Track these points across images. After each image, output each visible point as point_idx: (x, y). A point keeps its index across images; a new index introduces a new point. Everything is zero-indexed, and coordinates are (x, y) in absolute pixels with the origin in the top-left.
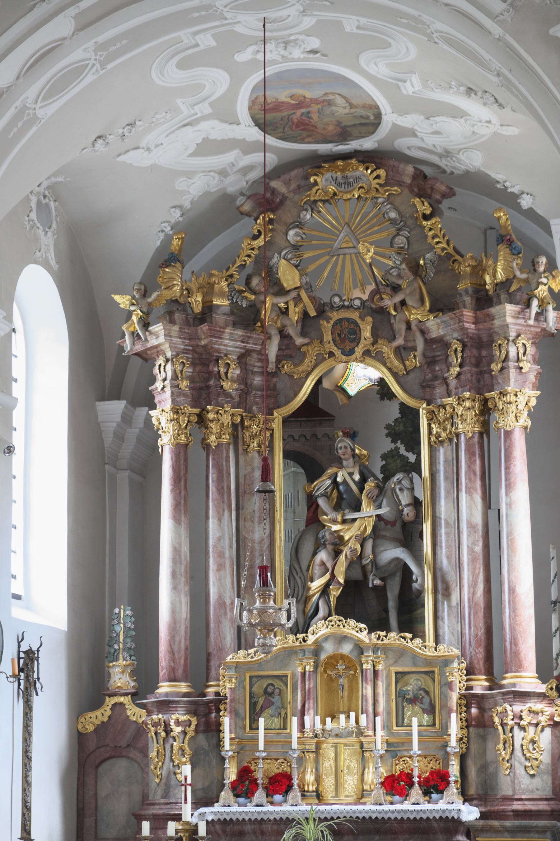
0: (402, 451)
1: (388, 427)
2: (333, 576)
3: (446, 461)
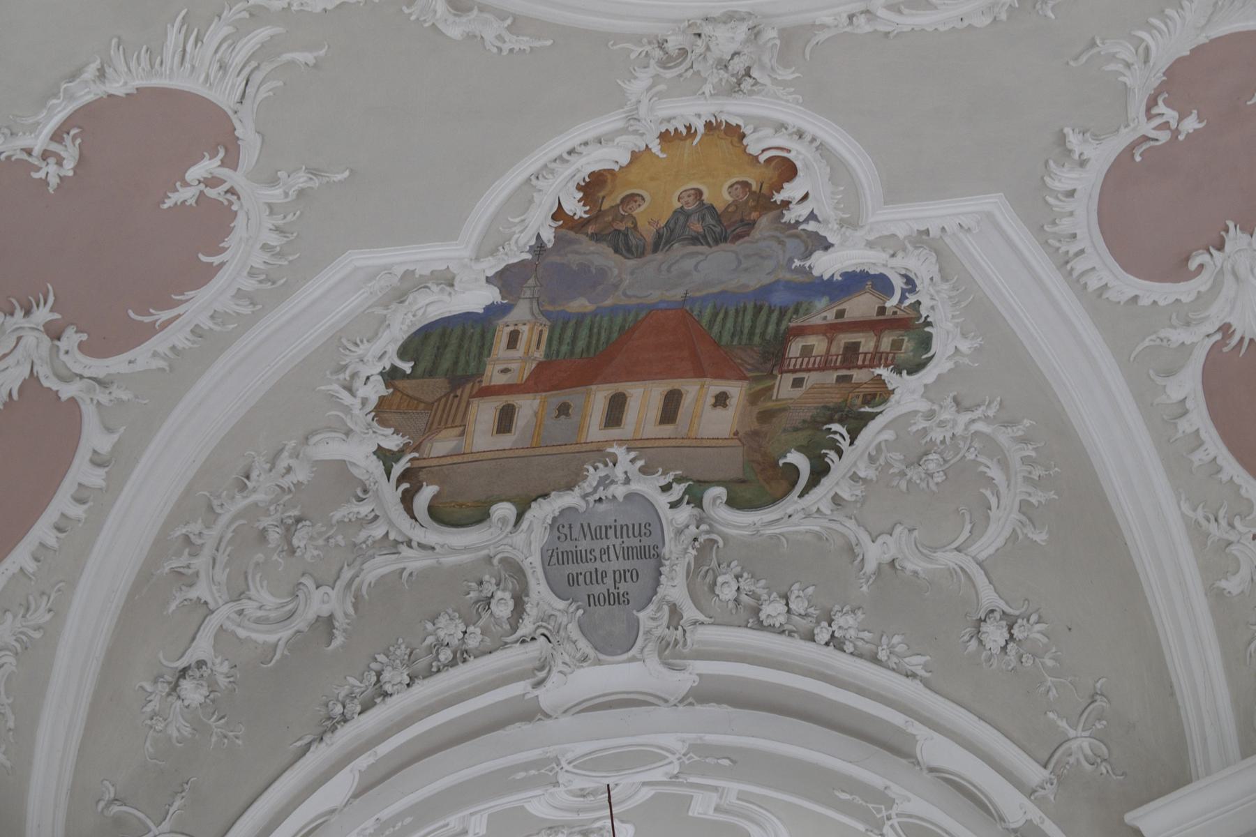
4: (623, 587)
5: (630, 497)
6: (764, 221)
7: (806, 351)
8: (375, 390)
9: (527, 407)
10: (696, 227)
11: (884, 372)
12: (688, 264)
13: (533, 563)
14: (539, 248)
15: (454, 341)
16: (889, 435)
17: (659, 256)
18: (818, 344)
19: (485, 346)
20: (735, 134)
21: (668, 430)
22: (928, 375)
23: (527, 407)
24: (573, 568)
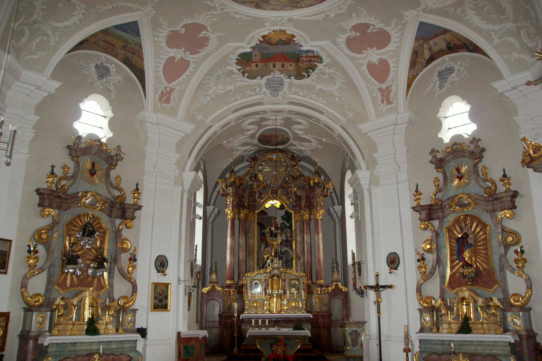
0: (285, 223)
1: (282, 217)
2: (271, 254)
3: (299, 226)
4: (277, 89)
5: (278, 77)
6: (292, 43)
7: (303, 60)
8: (235, 61)
9: (260, 65)
10: (281, 42)
11: (316, 63)
12: (282, 47)
13: (263, 85)
14: (257, 44)
15: (246, 56)
16: (319, 71)
17: (276, 46)
18: (305, 59)
19: (251, 56)
20: (284, 31)
21: (283, 69)
22: (323, 64)
23: (260, 65)
24: (270, 86)
